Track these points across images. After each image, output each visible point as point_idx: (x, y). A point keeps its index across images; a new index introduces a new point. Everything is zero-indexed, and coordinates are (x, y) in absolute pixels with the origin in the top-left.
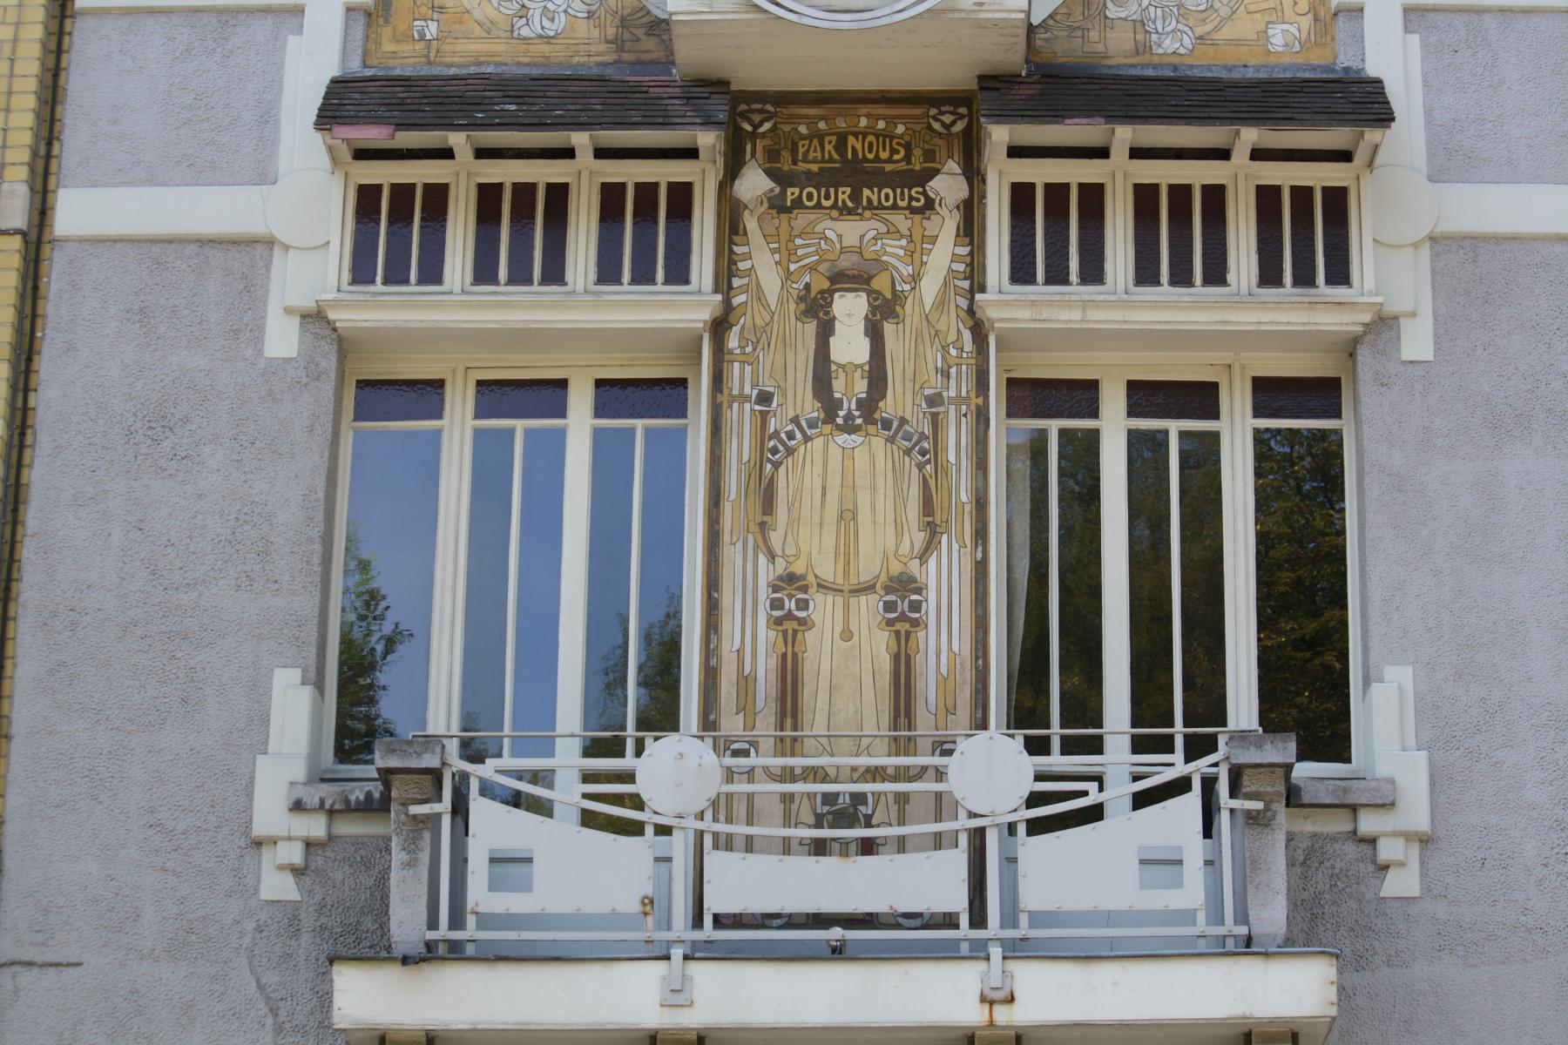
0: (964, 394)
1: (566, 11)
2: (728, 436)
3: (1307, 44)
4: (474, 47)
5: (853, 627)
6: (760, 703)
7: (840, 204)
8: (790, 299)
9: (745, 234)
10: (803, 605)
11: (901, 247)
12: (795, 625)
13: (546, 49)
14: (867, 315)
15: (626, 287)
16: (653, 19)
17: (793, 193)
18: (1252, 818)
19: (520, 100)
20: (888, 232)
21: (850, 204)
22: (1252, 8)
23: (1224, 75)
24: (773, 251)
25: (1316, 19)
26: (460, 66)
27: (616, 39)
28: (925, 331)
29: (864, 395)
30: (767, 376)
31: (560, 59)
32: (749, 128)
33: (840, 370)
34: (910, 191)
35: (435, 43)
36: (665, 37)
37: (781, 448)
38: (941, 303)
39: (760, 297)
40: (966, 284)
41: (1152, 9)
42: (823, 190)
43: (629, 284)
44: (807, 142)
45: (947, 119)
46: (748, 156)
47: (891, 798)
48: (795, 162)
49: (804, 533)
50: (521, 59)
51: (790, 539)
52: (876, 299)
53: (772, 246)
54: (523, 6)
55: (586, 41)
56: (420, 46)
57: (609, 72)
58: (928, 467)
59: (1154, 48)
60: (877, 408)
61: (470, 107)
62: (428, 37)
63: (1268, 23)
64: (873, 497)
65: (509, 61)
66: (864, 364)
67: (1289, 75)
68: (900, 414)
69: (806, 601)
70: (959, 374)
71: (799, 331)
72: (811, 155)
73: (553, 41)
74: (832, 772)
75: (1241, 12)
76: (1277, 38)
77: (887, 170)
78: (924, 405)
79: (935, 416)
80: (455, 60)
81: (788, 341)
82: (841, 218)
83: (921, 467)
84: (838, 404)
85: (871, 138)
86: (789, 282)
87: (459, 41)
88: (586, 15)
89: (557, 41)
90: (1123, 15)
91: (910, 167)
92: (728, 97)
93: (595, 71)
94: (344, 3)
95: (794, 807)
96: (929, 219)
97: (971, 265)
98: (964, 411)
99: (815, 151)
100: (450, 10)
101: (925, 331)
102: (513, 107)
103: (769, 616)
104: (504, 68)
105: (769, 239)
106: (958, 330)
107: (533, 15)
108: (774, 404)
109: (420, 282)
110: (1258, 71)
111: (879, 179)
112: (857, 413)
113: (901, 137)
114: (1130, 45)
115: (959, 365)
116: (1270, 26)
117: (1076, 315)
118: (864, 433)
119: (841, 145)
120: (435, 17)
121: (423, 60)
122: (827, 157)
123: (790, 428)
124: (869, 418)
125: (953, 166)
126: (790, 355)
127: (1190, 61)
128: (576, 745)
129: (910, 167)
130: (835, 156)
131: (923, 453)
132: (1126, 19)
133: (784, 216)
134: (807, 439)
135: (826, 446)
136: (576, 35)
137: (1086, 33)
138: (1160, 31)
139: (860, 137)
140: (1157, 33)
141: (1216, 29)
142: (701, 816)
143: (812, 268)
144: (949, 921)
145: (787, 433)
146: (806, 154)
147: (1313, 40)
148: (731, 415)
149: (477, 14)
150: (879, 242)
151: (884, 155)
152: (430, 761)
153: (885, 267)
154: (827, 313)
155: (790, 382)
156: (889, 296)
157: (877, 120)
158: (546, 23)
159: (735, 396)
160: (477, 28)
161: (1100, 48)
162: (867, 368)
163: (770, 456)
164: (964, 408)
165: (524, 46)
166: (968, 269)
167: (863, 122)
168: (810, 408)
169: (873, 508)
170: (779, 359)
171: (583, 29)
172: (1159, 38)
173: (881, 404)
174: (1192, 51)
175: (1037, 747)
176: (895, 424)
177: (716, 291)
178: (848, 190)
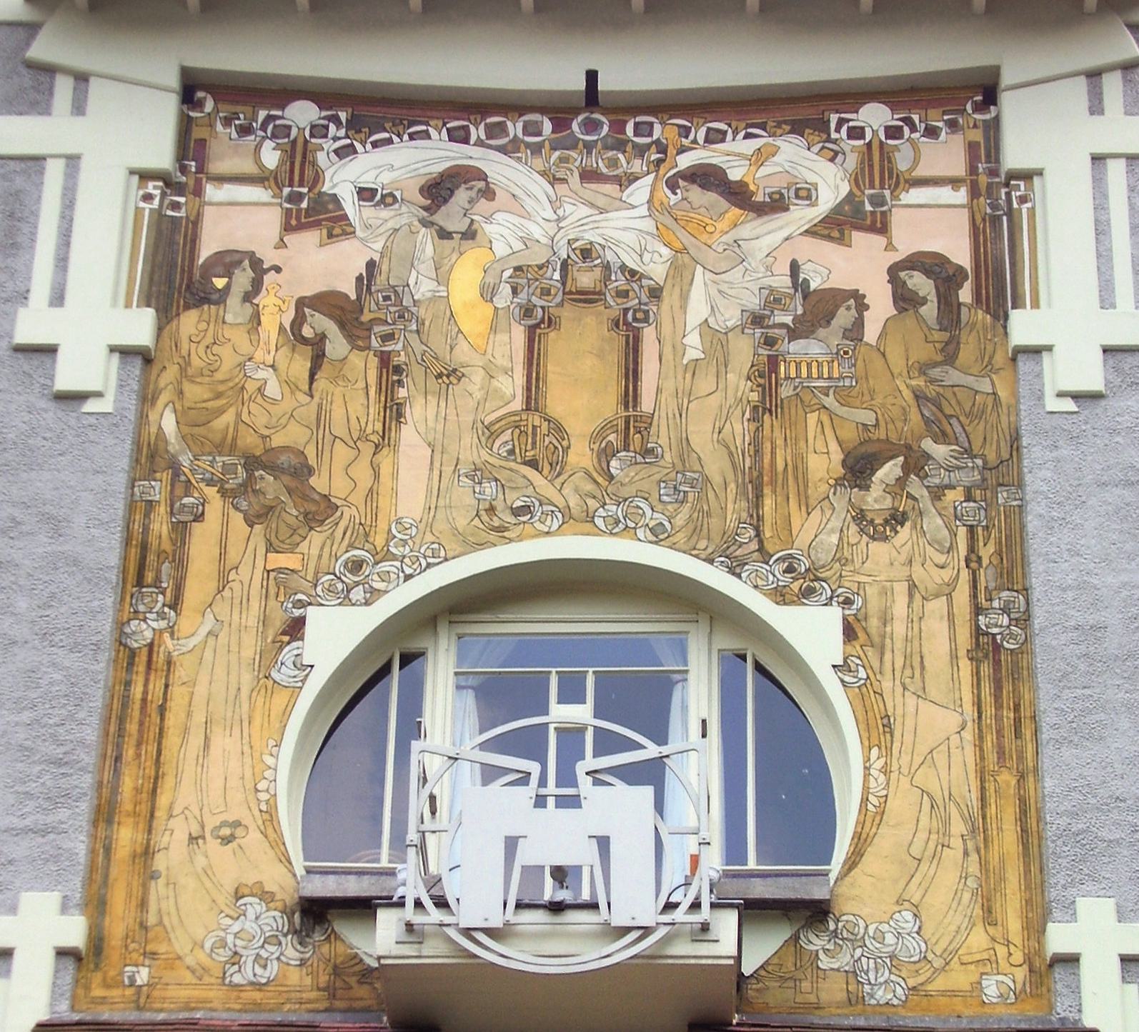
1: (278, 959)
4: (184, 993)
13: (257, 996)
22: (966, 959)
26: (171, 1011)
27: (328, 987)
41: (864, 960)
50: (232, 1006)
54: (236, 953)
55: (298, 989)
56: (129, 992)
59: (866, 999)
62: (139, 982)
63: (982, 974)
67: (1004, 1026)
73: (265, 988)
76: (991, 989)
80: (165, 1005)
88: (298, 963)
89: (269, 988)
90: (835, 966)
94: (55, 948)
100: (163, 957)
107: (245, 962)
110: (971, 1022)
114: (842, 996)
127: (902, 1012)
132: (838, 970)
136: (285, 983)
137: (798, 983)
138: (873, 982)
140: (870, 984)
141: (928, 981)
147: (1028, 990)
149: (190, 960)
158: (259, 970)
161: (812, 998)
165: (235, 994)
171: (295, 977)
172: (872, 989)
174: (906, 1001)
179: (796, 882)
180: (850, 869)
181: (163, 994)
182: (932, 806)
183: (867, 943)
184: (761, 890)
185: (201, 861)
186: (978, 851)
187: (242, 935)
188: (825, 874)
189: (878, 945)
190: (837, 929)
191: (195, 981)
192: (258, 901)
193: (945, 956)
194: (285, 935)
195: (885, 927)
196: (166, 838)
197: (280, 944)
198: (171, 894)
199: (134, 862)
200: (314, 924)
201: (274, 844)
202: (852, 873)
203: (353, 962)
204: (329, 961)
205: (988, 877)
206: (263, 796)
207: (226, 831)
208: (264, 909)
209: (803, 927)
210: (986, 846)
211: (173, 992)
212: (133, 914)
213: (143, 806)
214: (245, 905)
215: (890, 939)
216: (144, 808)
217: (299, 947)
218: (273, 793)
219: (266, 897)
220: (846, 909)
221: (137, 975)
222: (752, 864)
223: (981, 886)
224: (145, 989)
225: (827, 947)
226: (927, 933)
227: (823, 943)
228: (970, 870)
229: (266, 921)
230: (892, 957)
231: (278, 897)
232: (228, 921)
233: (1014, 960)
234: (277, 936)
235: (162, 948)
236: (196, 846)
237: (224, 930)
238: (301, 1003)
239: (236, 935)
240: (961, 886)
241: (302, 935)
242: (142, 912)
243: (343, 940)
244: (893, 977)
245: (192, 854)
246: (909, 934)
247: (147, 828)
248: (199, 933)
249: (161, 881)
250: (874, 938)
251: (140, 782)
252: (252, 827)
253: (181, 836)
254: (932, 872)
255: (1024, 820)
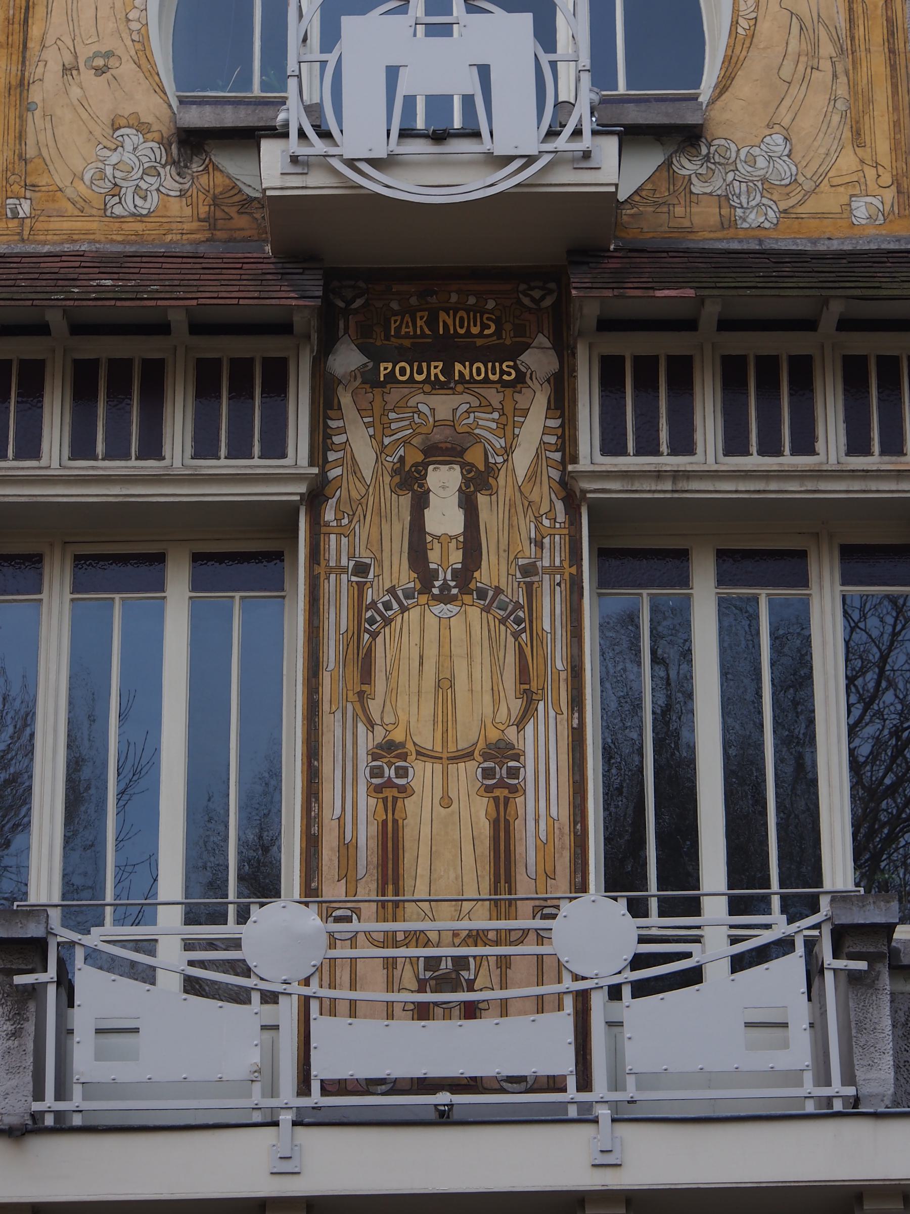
0: (557, 563)
1: (158, 190)
2: (326, 607)
3: (891, 217)
4: (67, 225)
5: (453, 794)
6: (361, 871)
7: (433, 378)
8: (385, 472)
9: (340, 408)
10: (402, 772)
11: (493, 420)
12: (394, 793)
13: (139, 227)
14: (461, 486)
15: (223, 462)
16: (245, 197)
17: (385, 368)
18: (854, 978)
19: (116, 276)
20: (480, 406)
21: (442, 378)
22: (836, 181)
23: (809, 247)
24: (367, 425)
25: (899, 192)
26: (55, 244)
28: (518, 503)
29: (460, 566)
30: (363, 547)
31: (153, 237)
32: (342, 305)
33: (435, 541)
34: (501, 366)
35: (29, 220)
36: (257, 216)
37: (378, 618)
38: (533, 476)
39: (355, 469)
40: (557, 456)
41: (736, 184)
42: (416, 365)
43: (226, 458)
44: (399, 318)
45: (537, 294)
46: (341, 333)
47: (492, 960)
48: (387, 337)
49: (402, 702)
50: (114, 237)
51: (388, 707)
52: (469, 472)
53: (366, 420)
54: (116, 185)
55: (179, 220)
56: (13, 224)
57: (202, 249)
58: (523, 635)
59: (739, 222)
60: (472, 578)
61: (66, 283)
62: (21, 215)
63: (852, 196)
64: (470, 665)
65: (103, 238)
66: (459, 535)
67: (873, 246)
68: (495, 583)
69: (406, 769)
70: (552, 543)
71: (394, 504)
72: (404, 330)
74: (433, 936)
75: (825, 186)
76: (861, 211)
77: (478, 344)
78: (518, 575)
79: (529, 585)
80: (49, 237)
81: (383, 514)
82: (434, 392)
83: (516, 635)
84: (434, 575)
85: (462, 313)
86: (384, 455)
87: (52, 219)
88: (178, 193)
90: (708, 190)
91: (501, 341)
92: (321, 272)
93: (189, 249)
95: (397, 973)
96: (520, 392)
97: (561, 437)
98: (558, 581)
99: (407, 327)
100: (43, 189)
101: (518, 503)
102: (109, 283)
103: (369, 785)
104: (98, 246)
105: (363, 413)
106: (551, 500)
107: (125, 194)
108: (371, 575)
109: (17, 457)
110: (843, 243)
111: (471, 353)
112: (452, 584)
113: (491, 312)
114: (714, 220)
115: (552, 535)
116: (853, 199)
117: (668, 486)
118: (460, 603)
119: (432, 322)
120: (28, 194)
121: (17, 238)
122: (419, 332)
123: (387, 598)
124: (464, 588)
125: (542, 340)
126: (386, 528)
127: (774, 235)
128: (177, 913)
129: (501, 341)
130: (428, 332)
131: (519, 621)
132: (710, 194)
133: (377, 391)
134: (404, 609)
135: (422, 615)
137: (671, 208)
138: (745, 205)
139: (451, 312)
140: (742, 207)
141: (801, 203)
142: (307, 982)
143: (406, 442)
144: (555, 1084)
145: (383, 603)
146: (398, 329)
147: (896, 212)
148: (329, 586)
149: (69, 192)
150: (472, 415)
151: (475, 330)
152: (34, 930)
153: (478, 439)
154: (421, 486)
155: (386, 554)
156: (482, 467)
157: (468, 296)
158: (139, 202)
159: (331, 568)
160: (70, 206)
161: (687, 223)
162: (461, 539)
163: (367, 626)
164: (558, 577)
166: (560, 440)
167: (454, 298)
168: (406, 578)
169: (470, 676)
170: (375, 530)
172: (744, 213)
173: (476, 574)
175: (637, 909)
176: (491, 593)
177: (311, 464)
178: (441, 364)
179: (663, 107)
180: (721, 94)
181: (45, 226)
182: (801, 28)
183: (739, 166)
184: (635, 116)
185: (75, 92)
186: (847, 74)
187: (120, 167)
188: (695, 98)
189: (750, 169)
190: (709, 153)
191: (77, 213)
192: (134, 132)
193: (815, 178)
194: (164, 166)
195: (756, 151)
196: (40, 70)
197: (159, 175)
198: (49, 126)
199: (10, 94)
200: (192, 154)
201: (148, 74)
202: (724, 97)
203: (232, 192)
204: (209, 191)
205: (856, 100)
206: (135, 26)
207: (100, 62)
208: (142, 140)
209: (676, 152)
210: (854, 68)
211: (56, 224)
212: (11, 145)
213: (16, 37)
214: (122, 136)
215: (761, 162)
216: (17, 39)
217: (177, 178)
218: (144, 22)
219: (142, 128)
220: (719, 132)
221: (18, 207)
222: (622, 89)
223: (850, 108)
224: (28, 221)
225: (700, 171)
226: (797, 157)
227: (695, 167)
228: (839, 92)
229: (144, 152)
230: (764, 180)
231: (155, 127)
232: (108, 153)
233: (881, 182)
234: (155, 167)
235: (43, 181)
236: (70, 78)
237: (101, 161)
238: (182, 234)
239: (114, 167)
240: (830, 109)
241: (180, 165)
242: (21, 145)
243: (221, 171)
244: (765, 201)
245: (67, 85)
246: (779, 158)
247: (21, 59)
248: (77, 164)
249: (37, 113)
250: (745, 162)
251: (11, 12)
252: (125, 58)
253: (54, 67)
254: (801, 96)
255: (891, 41)
